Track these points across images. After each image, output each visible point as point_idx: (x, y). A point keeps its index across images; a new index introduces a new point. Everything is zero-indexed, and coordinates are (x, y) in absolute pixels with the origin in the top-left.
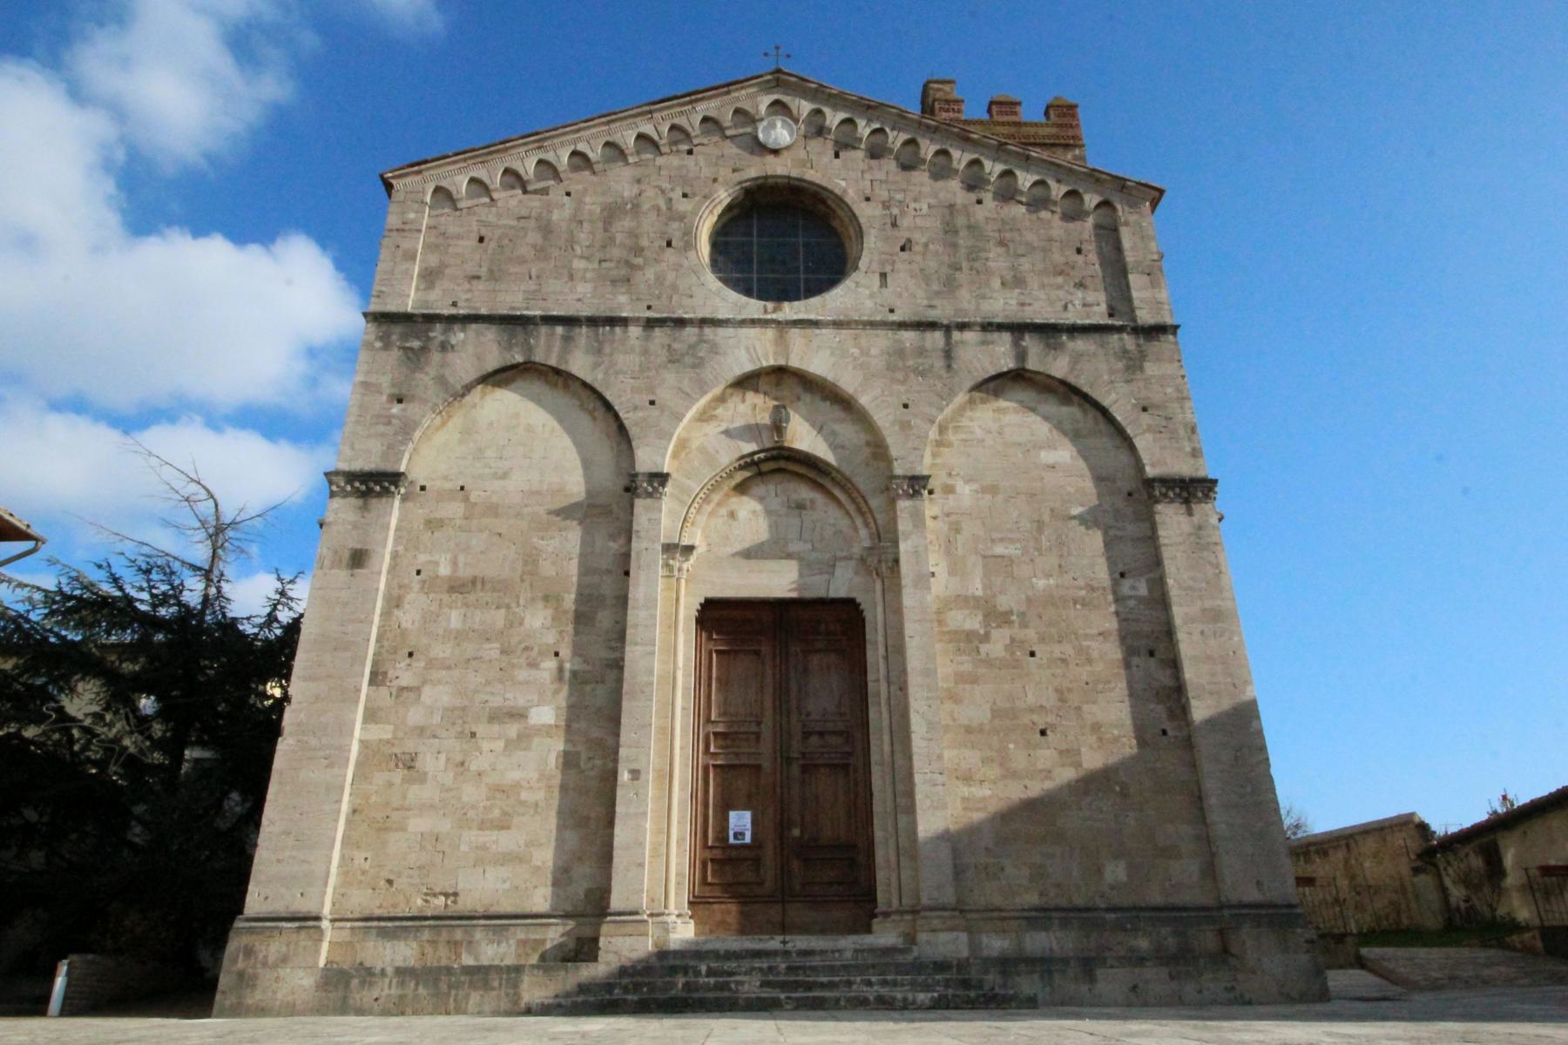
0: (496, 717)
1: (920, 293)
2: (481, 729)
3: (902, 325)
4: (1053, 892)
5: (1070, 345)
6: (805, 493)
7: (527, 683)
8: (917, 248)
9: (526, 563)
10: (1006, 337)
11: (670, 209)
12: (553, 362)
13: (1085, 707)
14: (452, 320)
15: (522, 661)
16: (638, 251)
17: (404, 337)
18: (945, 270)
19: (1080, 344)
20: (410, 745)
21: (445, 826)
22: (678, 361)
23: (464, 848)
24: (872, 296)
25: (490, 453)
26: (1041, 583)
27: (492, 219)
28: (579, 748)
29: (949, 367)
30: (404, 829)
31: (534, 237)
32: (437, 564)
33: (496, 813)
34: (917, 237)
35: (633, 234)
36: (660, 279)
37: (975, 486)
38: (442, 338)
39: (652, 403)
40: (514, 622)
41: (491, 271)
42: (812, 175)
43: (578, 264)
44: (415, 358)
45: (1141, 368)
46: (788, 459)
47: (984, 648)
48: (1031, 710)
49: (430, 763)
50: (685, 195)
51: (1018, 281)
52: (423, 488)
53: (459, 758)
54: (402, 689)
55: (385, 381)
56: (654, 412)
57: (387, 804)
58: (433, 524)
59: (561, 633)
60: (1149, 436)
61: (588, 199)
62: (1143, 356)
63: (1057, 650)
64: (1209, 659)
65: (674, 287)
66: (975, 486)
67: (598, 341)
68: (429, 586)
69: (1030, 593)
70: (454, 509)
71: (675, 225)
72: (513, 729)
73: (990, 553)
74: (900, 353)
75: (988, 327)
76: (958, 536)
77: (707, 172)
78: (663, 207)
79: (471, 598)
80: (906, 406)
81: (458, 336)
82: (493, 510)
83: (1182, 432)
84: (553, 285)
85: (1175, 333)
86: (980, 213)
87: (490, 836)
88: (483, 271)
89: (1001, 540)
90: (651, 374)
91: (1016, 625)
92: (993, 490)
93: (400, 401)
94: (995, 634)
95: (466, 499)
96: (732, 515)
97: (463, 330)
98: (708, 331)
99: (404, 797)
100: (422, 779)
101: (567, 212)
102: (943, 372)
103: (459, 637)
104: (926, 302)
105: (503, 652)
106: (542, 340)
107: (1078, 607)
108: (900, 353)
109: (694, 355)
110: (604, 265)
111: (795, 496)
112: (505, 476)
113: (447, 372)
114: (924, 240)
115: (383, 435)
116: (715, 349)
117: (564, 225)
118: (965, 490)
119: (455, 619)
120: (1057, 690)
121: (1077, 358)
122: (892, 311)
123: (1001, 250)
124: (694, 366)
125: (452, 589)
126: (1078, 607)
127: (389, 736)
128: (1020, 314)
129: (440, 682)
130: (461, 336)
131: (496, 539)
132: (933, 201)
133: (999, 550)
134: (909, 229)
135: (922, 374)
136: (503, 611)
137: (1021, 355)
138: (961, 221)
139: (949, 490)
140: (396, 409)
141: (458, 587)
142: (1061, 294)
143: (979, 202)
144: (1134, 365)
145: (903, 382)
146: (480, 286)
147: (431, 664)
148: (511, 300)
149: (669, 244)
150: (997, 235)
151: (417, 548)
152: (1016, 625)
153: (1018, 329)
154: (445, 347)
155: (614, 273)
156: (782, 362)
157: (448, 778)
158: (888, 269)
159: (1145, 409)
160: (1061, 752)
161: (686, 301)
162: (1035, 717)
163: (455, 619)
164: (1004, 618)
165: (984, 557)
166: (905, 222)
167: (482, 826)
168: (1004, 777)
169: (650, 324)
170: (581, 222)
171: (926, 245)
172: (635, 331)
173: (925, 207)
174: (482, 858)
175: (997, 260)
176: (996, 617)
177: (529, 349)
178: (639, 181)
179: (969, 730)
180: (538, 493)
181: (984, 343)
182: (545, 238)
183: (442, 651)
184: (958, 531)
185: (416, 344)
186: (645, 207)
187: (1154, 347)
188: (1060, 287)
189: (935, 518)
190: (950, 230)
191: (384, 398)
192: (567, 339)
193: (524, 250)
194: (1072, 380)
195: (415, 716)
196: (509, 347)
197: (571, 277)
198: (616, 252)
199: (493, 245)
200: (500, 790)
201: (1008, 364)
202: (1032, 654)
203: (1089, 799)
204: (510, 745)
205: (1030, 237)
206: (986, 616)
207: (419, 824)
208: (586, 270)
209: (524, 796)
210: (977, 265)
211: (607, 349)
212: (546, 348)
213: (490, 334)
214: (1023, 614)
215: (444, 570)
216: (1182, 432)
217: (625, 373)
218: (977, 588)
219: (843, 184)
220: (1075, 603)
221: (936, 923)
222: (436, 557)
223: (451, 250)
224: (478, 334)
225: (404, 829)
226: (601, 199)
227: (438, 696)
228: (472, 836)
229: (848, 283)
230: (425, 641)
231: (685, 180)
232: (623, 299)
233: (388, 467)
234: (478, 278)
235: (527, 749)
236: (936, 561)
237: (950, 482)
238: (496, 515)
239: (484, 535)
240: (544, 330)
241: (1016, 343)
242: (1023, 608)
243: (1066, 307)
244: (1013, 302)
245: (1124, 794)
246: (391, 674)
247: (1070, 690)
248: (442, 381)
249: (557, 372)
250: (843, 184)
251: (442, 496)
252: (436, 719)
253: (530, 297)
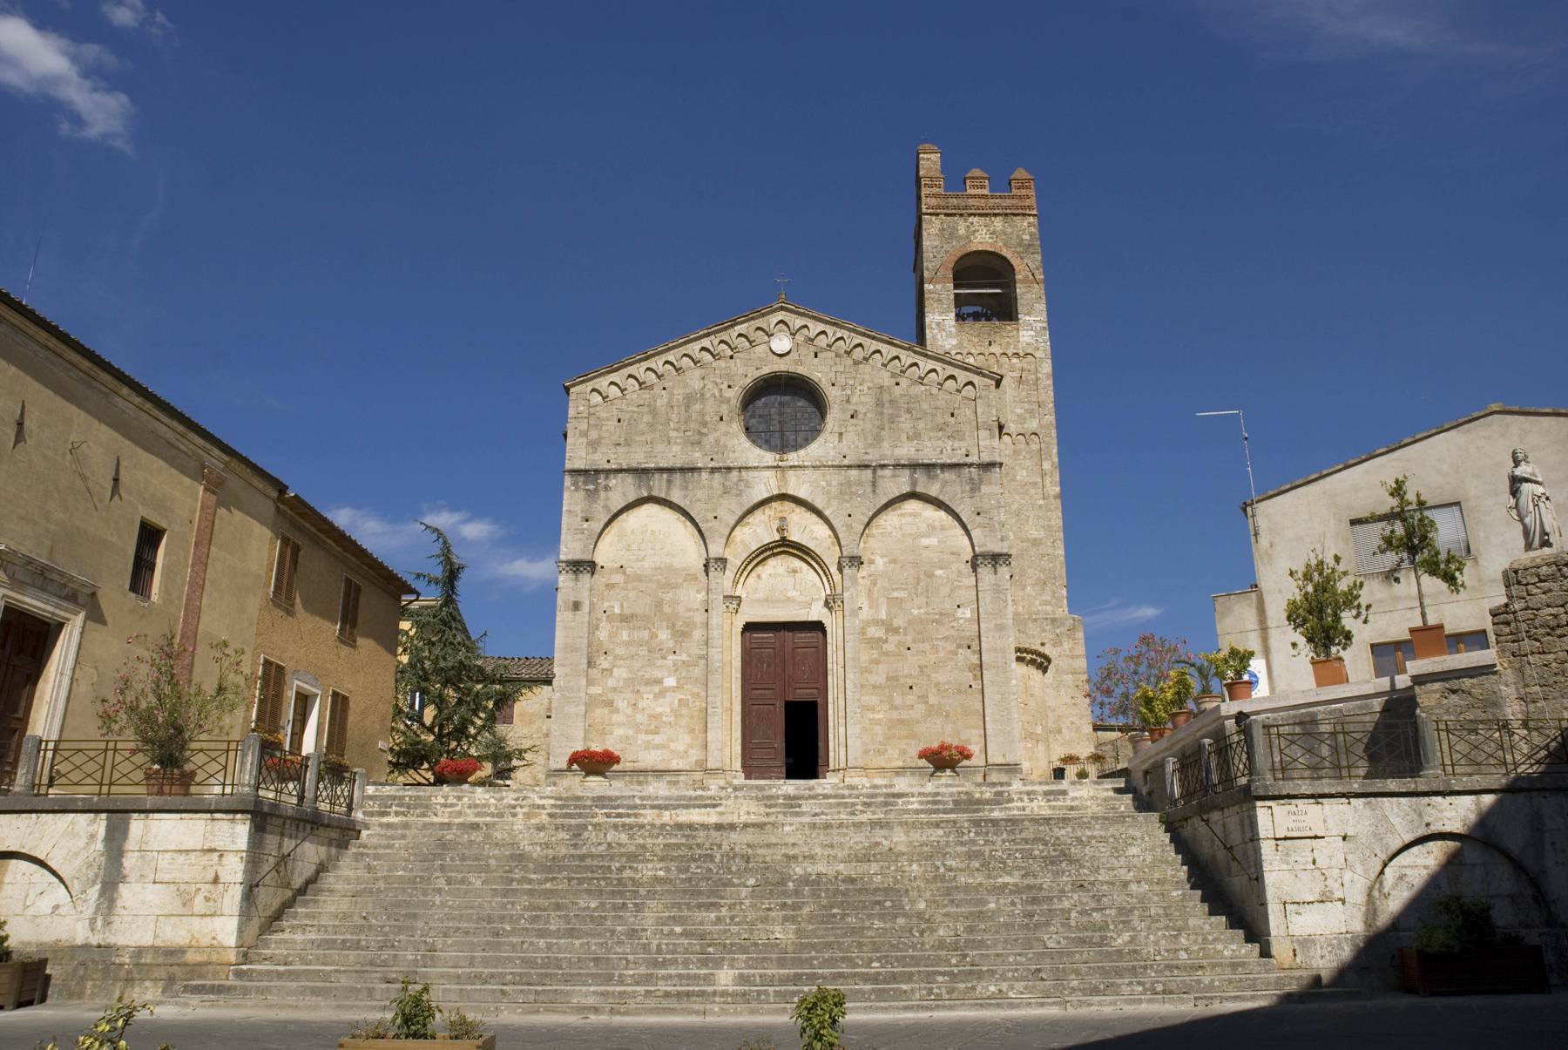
0: (649, 682)
1: (861, 445)
2: (643, 689)
3: (849, 467)
4: (909, 760)
5: (941, 476)
6: (797, 563)
7: (661, 666)
8: (860, 416)
9: (656, 606)
10: (907, 472)
11: (721, 396)
12: (663, 495)
13: (933, 675)
14: (608, 472)
15: (659, 656)
16: (705, 424)
17: (586, 483)
18: (875, 430)
19: (949, 475)
20: (610, 696)
21: (631, 732)
22: (729, 492)
23: (639, 742)
24: (834, 448)
25: (634, 547)
26: (915, 612)
27: (624, 407)
28: (689, 697)
29: (874, 491)
30: (611, 734)
31: (647, 418)
32: (613, 607)
33: (652, 727)
34: (862, 410)
35: (702, 413)
36: (717, 441)
37: (886, 559)
38: (604, 483)
39: (715, 518)
40: (653, 636)
41: (626, 440)
42: (801, 370)
43: (673, 434)
44: (592, 495)
45: (979, 490)
46: (788, 546)
47: (885, 646)
48: (906, 677)
49: (621, 704)
50: (729, 387)
51: (916, 436)
52: (602, 567)
53: (634, 702)
54: (603, 670)
55: (578, 509)
56: (716, 523)
57: (603, 722)
58: (610, 586)
59: (676, 642)
60: (979, 530)
61: (676, 392)
62: (981, 483)
63: (921, 646)
64: (995, 650)
65: (725, 446)
66: (886, 559)
67: (686, 481)
68: (610, 619)
69: (910, 617)
70: (618, 578)
71: (725, 406)
72: (656, 689)
74: (849, 484)
75: (896, 466)
77: (741, 371)
78: (717, 395)
79: (631, 624)
80: (850, 516)
81: (613, 481)
82: (639, 578)
83: (997, 526)
84: (660, 447)
85: (1000, 467)
86: (897, 391)
87: (650, 737)
88: (622, 441)
89: (897, 589)
90: (715, 501)
92: (894, 561)
93: (587, 520)
95: (624, 573)
96: (759, 576)
97: (615, 478)
98: (744, 473)
99: (610, 719)
100: (618, 711)
101: (665, 400)
102: (871, 495)
103: (628, 644)
104: (863, 451)
105: (649, 651)
106: (656, 482)
108: (849, 484)
109: (737, 489)
110: (687, 433)
111: (791, 566)
112: (643, 559)
113: (609, 503)
114: (864, 411)
115: (581, 540)
116: (748, 485)
117: (663, 408)
118: (880, 561)
119: (625, 635)
121: (945, 484)
122: (844, 457)
123: (908, 416)
124: (737, 495)
125: (622, 621)
127: (600, 692)
128: (916, 457)
129: (620, 666)
130: (614, 481)
131: (640, 594)
132: (871, 385)
133: (896, 594)
134: (856, 404)
135: (859, 496)
136: (647, 631)
137: (914, 483)
138: (886, 397)
139: (872, 562)
140: (585, 525)
141: (625, 619)
142: (940, 442)
143: (897, 384)
144: (975, 488)
145: (848, 502)
146: (621, 449)
147: (616, 657)
148: (638, 458)
149: (721, 419)
150: (906, 406)
151: (602, 599)
153: (914, 466)
154: (607, 488)
155: (692, 438)
156: (783, 491)
157: (629, 711)
158: (843, 430)
159: (978, 514)
161: (731, 455)
162: (908, 680)
163: (625, 635)
164: (896, 631)
166: (854, 399)
167: (647, 732)
169: (713, 470)
170: (672, 407)
171: (865, 414)
172: (705, 475)
173: (866, 389)
174: (648, 747)
175: (905, 423)
176: (891, 629)
177: (650, 488)
178: (703, 378)
179: (875, 687)
180: (659, 568)
181: (894, 476)
182: (654, 418)
183: (621, 651)
184: (875, 585)
185: (591, 487)
186: (707, 396)
187: (986, 476)
188: (939, 439)
189: (863, 577)
190: (879, 403)
191: (579, 519)
192: (669, 482)
193: (643, 427)
194: (941, 498)
195: (611, 683)
196: (640, 487)
197: (669, 443)
198: (693, 425)
199: (625, 423)
200: (651, 717)
201: (906, 489)
202: (909, 649)
204: (656, 696)
205: (925, 406)
206: (887, 631)
207: (619, 732)
208: (677, 437)
209: (664, 719)
210: (892, 426)
211: (691, 487)
212: (658, 486)
213: (629, 479)
215: (617, 611)
216: (997, 526)
217: (699, 500)
218: (883, 615)
219: (819, 375)
221: (853, 774)
222: (612, 604)
223: (604, 428)
224: (623, 479)
225: (611, 734)
226: (683, 391)
227: (621, 673)
228: (642, 737)
229: (820, 439)
230: (612, 646)
231: (729, 376)
232: (697, 455)
233: (587, 557)
234: (619, 444)
235: (664, 697)
236: (863, 601)
237: (873, 557)
238: (641, 581)
239: (635, 592)
240: (657, 476)
241: (911, 476)
242: (906, 625)
243: (942, 451)
244: (913, 449)
246: (598, 662)
247: (926, 666)
248: (606, 507)
249: (665, 500)
250: (819, 375)
251: (613, 571)
252: (621, 684)
253: (649, 455)
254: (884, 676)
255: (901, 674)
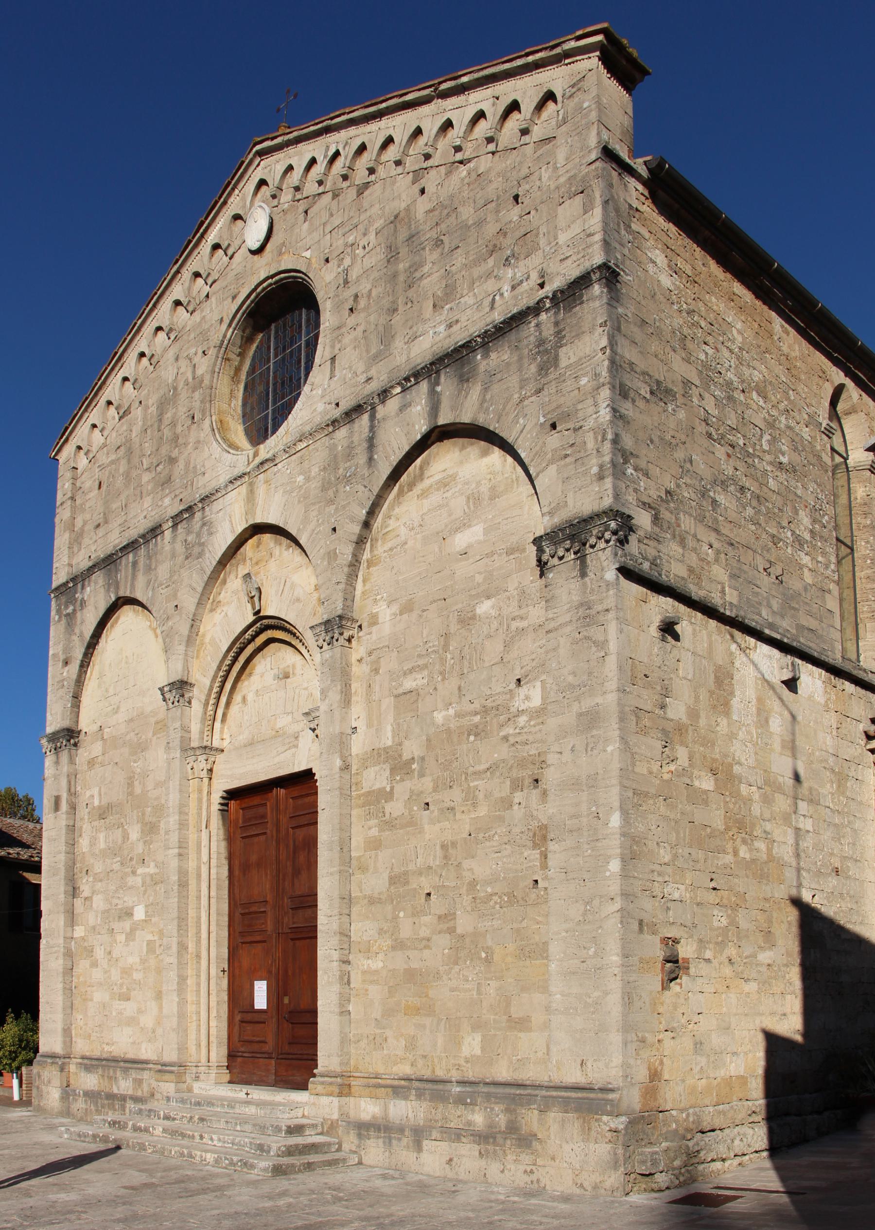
13: (466, 864)
26: (439, 717)
37: (395, 608)
73: (401, 691)
76: (377, 678)
89: (412, 670)
91: (416, 773)
92: (407, 608)
94: (398, 788)
107: (472, 738)
120: (444, 847)
126: (472, 738)
133: (409, 684)
139: (374, 620)
152: (416, 773)
160: (440, 917)
165: (397, 696)
168: (394, 948)
184: (376, 671)
189: (359, 661)
203: (457, 968)
214: (423, 759)
220: (469, 735)
245: (488, 961)
247: (454, 844)
254: (386, 876)
255: (411, 867)
